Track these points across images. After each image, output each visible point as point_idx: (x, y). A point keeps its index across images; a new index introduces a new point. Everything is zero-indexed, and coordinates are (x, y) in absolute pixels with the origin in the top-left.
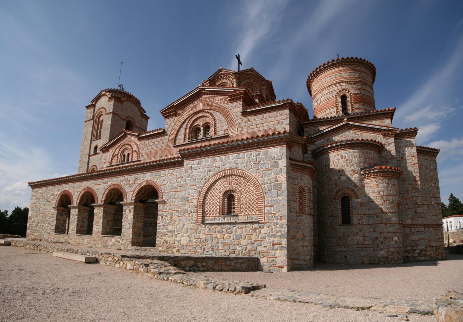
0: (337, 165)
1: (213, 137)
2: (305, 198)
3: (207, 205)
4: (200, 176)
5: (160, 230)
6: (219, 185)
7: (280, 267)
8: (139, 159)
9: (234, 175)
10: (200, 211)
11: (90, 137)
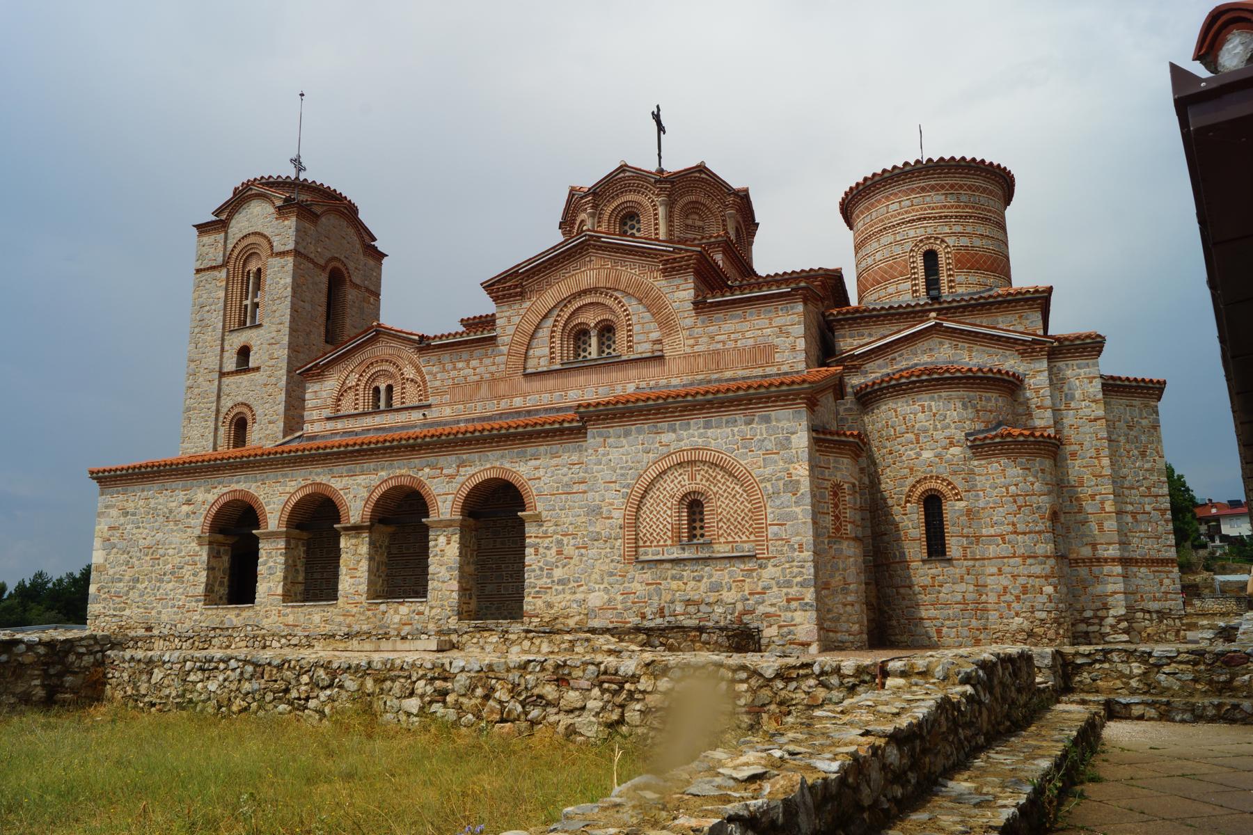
0: (913, 426)
4: (627, 462)
5: (532, 580)
6: (668, 482)
7: (803, 644)
8: (425, 403)
9: (702, 461)
11: (221, 318)
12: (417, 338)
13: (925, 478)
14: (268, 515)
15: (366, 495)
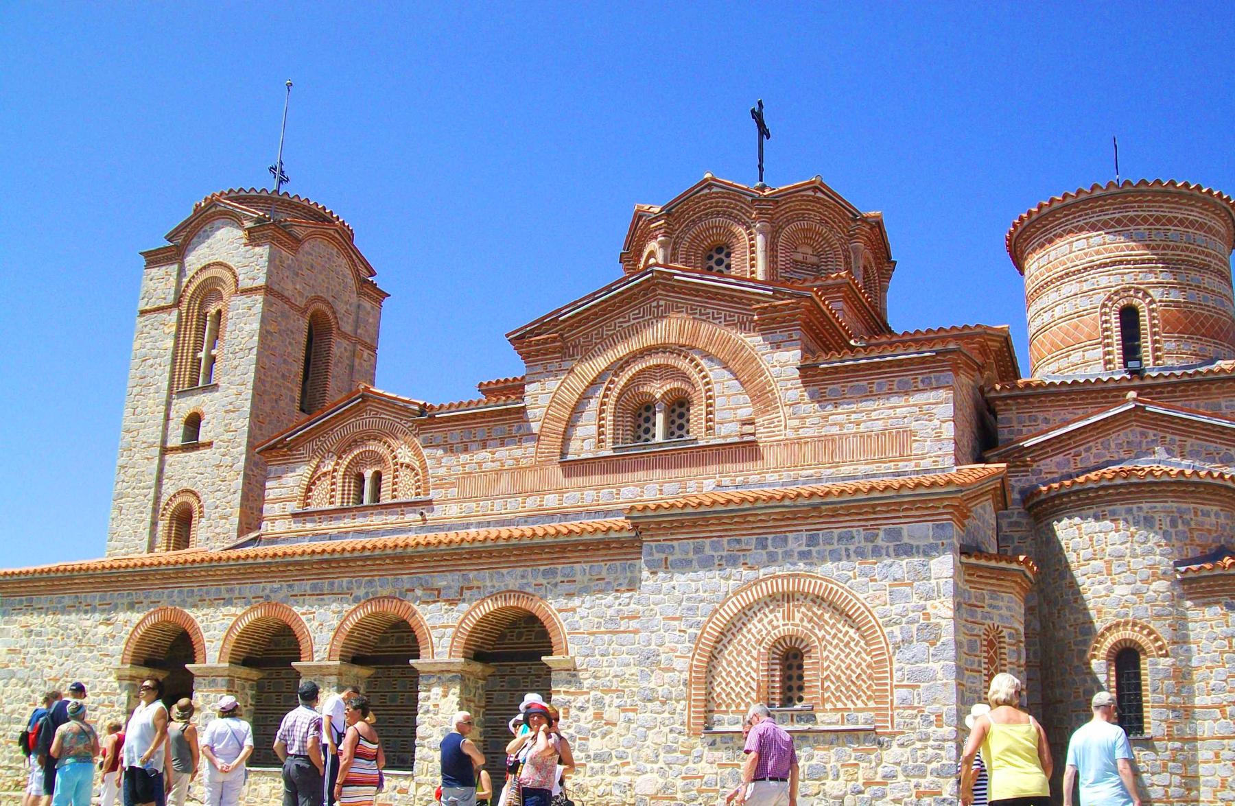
1: (702, 443)
2: (1003, 662)
3: (719, 679)
4: (697, 591)
8: (422, 498)
10: (698, 693)
11: (167, 375)
12: (416, 408)
13: (1118, 625)
14: (207, 644)
15: (336, 623)
